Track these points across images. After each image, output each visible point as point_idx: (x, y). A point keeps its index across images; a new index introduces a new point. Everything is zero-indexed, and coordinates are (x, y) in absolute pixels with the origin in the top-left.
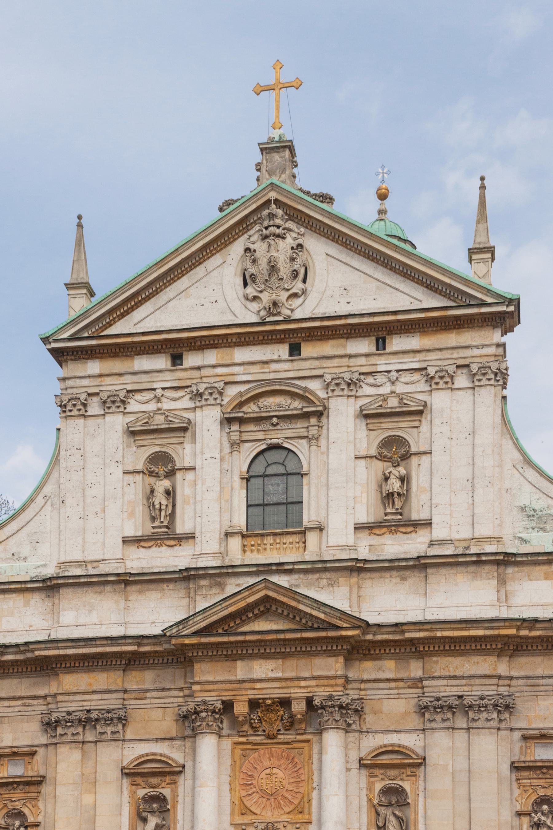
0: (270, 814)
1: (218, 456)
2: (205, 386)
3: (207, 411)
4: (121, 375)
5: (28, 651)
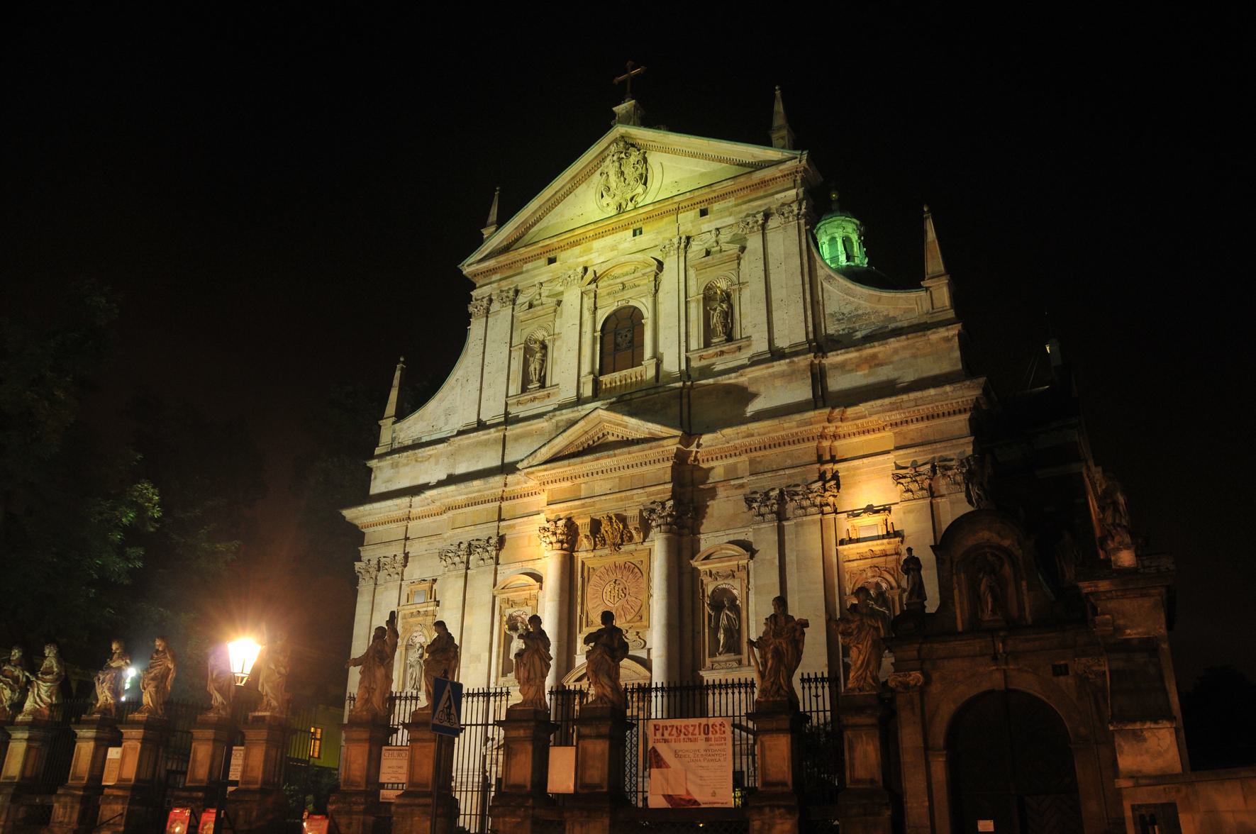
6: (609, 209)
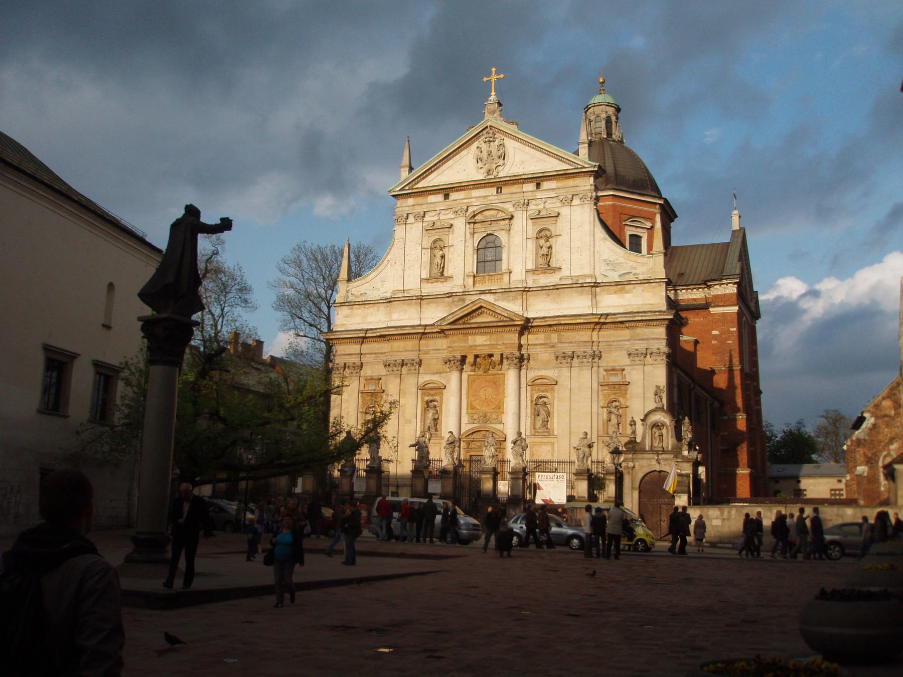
2: (458, 208)
4: (422, 205)
5: (376, 332)
6: (482, 171)
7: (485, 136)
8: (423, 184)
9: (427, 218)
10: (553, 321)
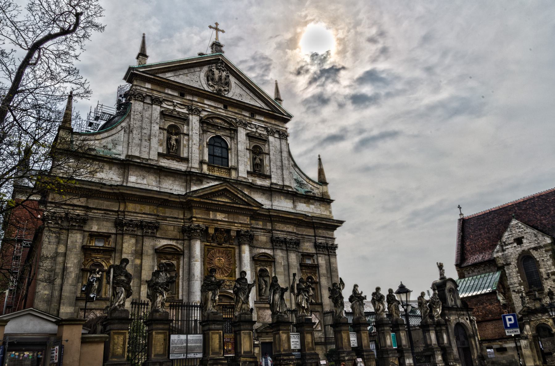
0: (219, 276)
1: (198, 133)
3: (194, 116)
6: (211, 88)
7: (220, 65)
8: (160, 75)
9: (164, 105)
10: (275, 213)
